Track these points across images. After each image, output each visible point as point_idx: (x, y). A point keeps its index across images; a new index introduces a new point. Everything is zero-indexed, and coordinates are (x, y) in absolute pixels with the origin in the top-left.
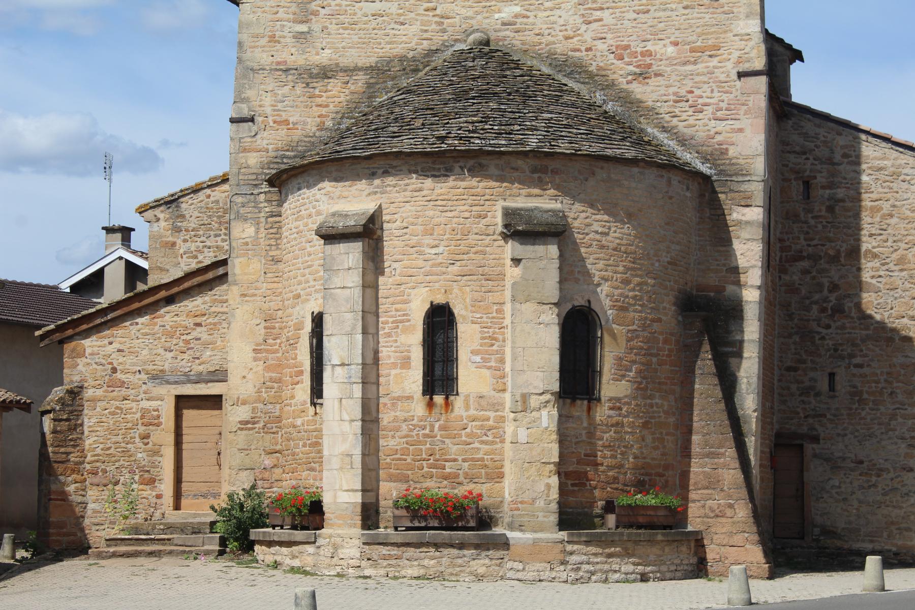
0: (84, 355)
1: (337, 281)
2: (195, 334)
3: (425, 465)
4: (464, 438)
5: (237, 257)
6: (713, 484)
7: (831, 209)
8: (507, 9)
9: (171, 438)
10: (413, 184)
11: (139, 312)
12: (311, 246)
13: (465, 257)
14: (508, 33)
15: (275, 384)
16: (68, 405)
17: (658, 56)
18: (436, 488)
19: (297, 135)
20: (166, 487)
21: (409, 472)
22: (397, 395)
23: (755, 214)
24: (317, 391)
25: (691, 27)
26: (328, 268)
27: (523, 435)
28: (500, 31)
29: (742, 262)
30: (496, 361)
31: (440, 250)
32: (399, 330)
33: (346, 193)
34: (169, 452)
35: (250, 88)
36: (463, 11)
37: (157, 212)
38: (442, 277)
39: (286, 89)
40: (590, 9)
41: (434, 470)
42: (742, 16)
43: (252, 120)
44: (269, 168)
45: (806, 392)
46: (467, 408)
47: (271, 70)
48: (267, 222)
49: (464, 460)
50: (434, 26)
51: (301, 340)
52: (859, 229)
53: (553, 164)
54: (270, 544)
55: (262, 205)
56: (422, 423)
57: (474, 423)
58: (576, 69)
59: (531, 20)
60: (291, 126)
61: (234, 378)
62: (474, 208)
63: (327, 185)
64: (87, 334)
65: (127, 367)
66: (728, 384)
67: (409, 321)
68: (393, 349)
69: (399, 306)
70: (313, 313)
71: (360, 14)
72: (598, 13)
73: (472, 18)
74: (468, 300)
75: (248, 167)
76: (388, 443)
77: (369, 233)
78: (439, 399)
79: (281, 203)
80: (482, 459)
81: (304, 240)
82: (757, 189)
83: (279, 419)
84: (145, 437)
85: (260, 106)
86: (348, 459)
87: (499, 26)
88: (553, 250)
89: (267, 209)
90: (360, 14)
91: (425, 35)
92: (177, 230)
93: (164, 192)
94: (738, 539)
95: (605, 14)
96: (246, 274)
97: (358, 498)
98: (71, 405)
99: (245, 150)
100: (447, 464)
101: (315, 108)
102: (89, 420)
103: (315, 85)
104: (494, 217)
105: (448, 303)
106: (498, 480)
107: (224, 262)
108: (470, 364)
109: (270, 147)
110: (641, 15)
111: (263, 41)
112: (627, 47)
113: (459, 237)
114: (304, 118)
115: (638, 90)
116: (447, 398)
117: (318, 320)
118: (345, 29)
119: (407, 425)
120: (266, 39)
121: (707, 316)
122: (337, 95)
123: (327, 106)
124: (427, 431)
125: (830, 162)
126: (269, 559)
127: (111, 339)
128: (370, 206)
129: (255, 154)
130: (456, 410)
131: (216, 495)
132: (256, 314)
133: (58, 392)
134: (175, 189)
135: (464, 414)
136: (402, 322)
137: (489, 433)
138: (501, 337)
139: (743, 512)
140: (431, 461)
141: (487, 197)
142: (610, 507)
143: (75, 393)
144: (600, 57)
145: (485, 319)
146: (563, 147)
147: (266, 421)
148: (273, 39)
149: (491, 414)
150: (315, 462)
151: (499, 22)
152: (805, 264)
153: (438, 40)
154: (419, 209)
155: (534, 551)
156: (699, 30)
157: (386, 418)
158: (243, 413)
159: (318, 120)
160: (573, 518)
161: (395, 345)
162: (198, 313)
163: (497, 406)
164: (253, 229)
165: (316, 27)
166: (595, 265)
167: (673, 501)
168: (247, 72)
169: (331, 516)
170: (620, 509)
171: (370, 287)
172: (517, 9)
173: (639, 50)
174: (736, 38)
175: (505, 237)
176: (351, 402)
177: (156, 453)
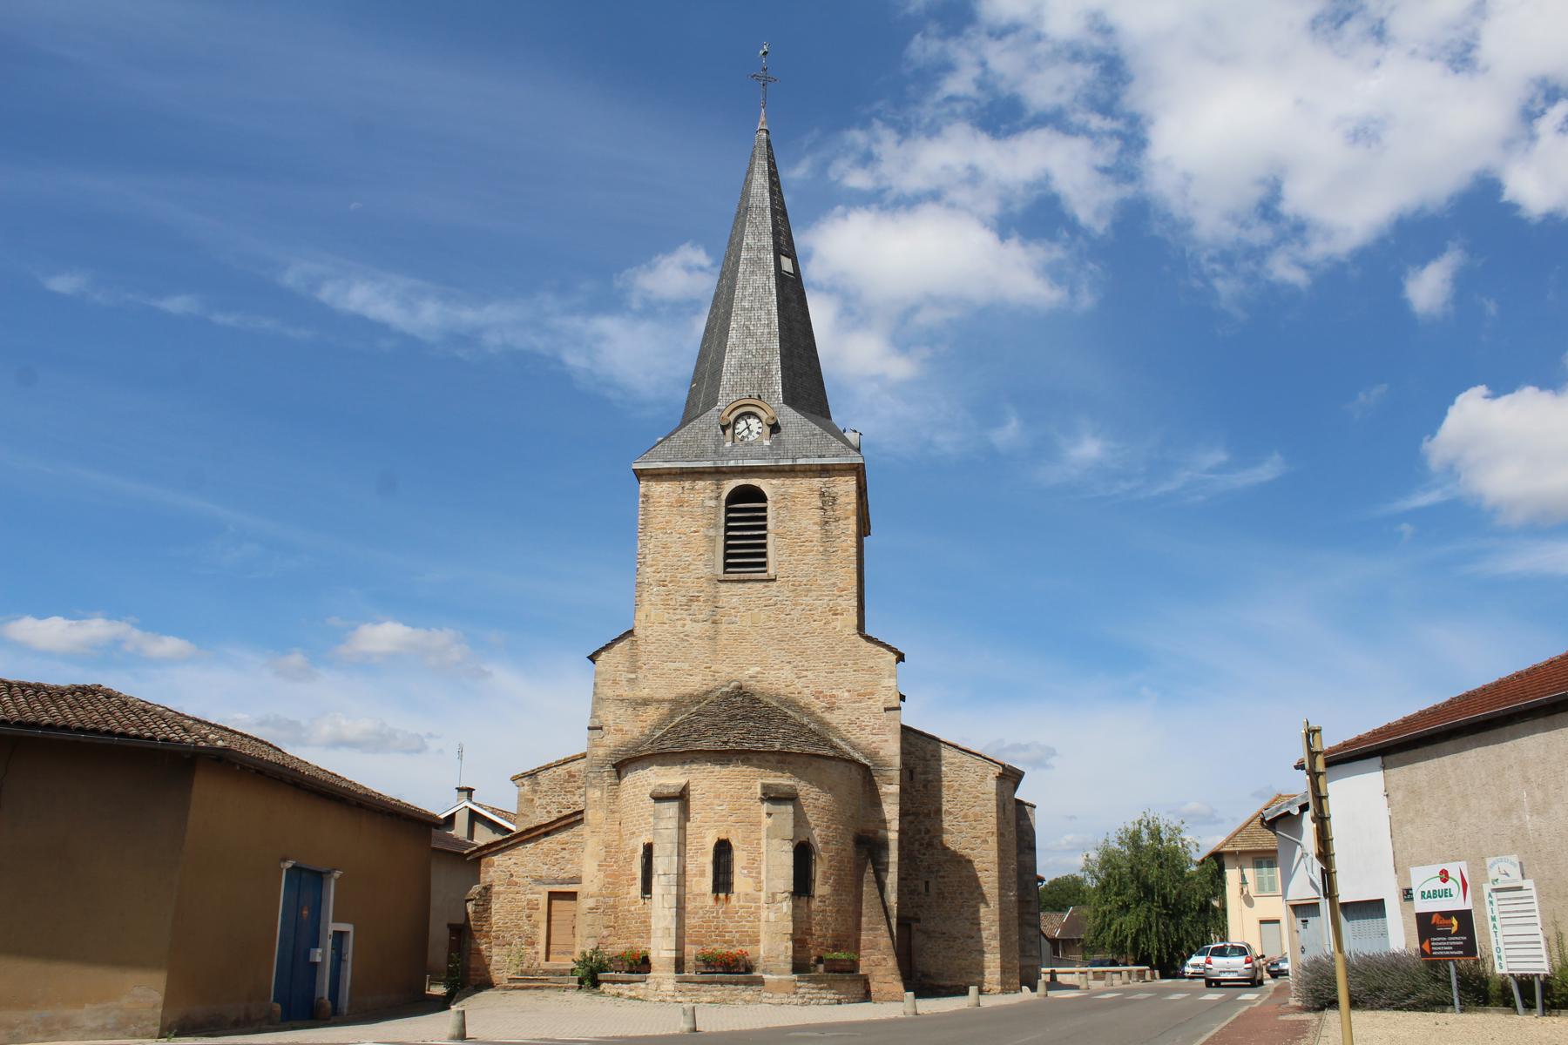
1: (662, 824)
6: (874, 946)
7: (925, 786)
9: (545, 918)
11: (528, 841)
15: (614, 882)
18: (721, 949)
19: (628, 737)
20: (541, 948)
23: (895, 789)
24: (647, 888)
27: (772, 917)
29: (888, 817)
34: (544, 926)
37: (525, 781)
45: (911, 893)
52: (940, 797)
53: (789, 759)
54: (614, 982)
58: (792, 704)
61: (585, 882)
63: (655, 768)
64: (496, 853)
66: (881, 887)
76: (691, 921)
77: (682, 796)
78: (722, 895)
79: (619, 777)
82: (896, 774)
83: (614, 907)
84: (529, 916)
88: (790, 808)
92: (535, 791)
93: (528, 769)
94: (889, 979)
95: (809, 673)
97: (673, 954)
102: (495, 906)
107: (581, 812)
114: (631, 728)
115: (828, 717)
117: (648, 849)
121: (869, 847)
122: (652, 715)
125: (925, 759)
126: (614, 991)
128: (683, 781)
131: (572, 953)
133: (476, 888)
134: (535, 767)
139: (892, 962)
142: (820, 960)
143: (487, 889)
144: (807, 698)
146: (795, 749)
147: (609, 908)
150: (646, 931)
152: (910, 818)
153: (712, 685)
155: (779, 986)
157: (689, 906)
158: (591, 903)
160: (799, 967)
163: (756, 900)
165: (641, 676)
166: (812, 818)
167: (852, 956)
168: (598, 700)
170: (825, 962)
171: (682, 828)
175: (762, 800)
177: (535, 926)
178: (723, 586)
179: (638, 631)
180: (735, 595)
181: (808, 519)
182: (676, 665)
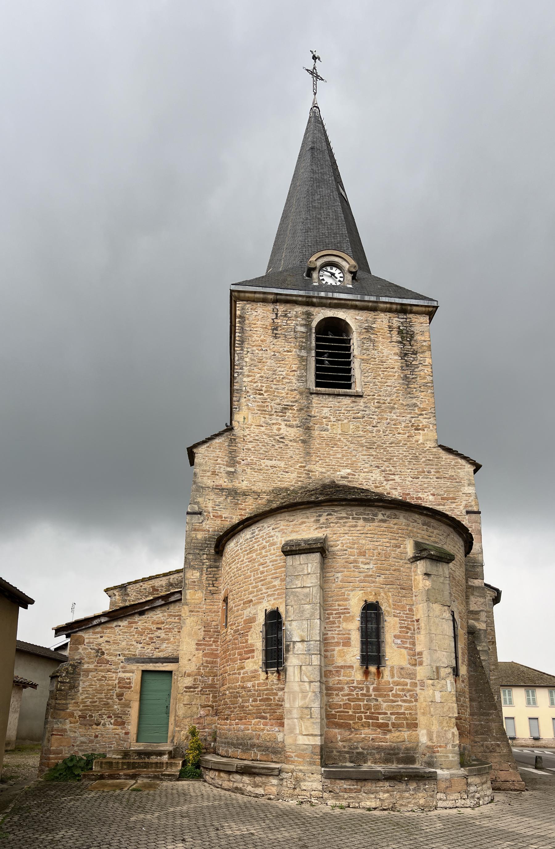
0: (83, 643)
2: (157, 634)
3: (364, 717)
4: (391, 698)
5: (188, 589)
8: (343, 471)
10: (350, 522)
12: (264, 567)
13: (387, 572)
14: (344, 482)
16: (71, 674)
17: (425, 500)
21: (351, 722)
22: (340, 665)
25: (441, 487)
26: (288, 576)
28: (340, 481)
30: (410, 644)
31: (371, 566)
32: (341, 619)
33: (298, 529)
35: (200, 497)
36: (320, 470)
38: (372, 585)
39: (222, 499)
40: (388, 474)
41: (371, 721)
42: (466, 485)
43: (200, 513)
44: (209, 541)
46: (393, 676)
47: (213, 488)
48: (207, 571)
49: (391, 714)
50: (304, 475)
51: (252, 629)
55: (205, 561)
56: (360, 686)
57: (398, 687)
59: (357, 477)
60: (223, 519)
62: (392, 541)
65: (111, 651)
67: (349, 613)
68: (336, 632)
69: (341, 603)
70: (266, 610)
71: (263, 465)
72: (393, 476)
73: (325, 473)
74: (391, 601)
75: (197, 539)
78: (373, 669)
80: (404, 714)
81: (256, 564)
85: (206, 507)
86: (306, 711)
87: (339, 479)
89: (207, 564)
90: (263, 465)
91: (299, 479)
95: (396, 477)
96: (193, 599)
98: (72, 674)
99: (195, 530)
100: (380, 716)
101: (238, 511)
103: (239, 498)
104: (405, 548)
105: (377, 602)
106: (414, 729)
108: (393, 645)
109: (211, 529)
110: (415, 479)
111: (209, 474)
112: (409, 494)
113: (383, 558)
116: (378, 668)
118: (256, 472)
119: (349, 687)
120: (210, 473)
123: (245, 510)
124: (364, 692)
127: (102, 635)
129: (201, 533)
130: (385, 677)
132: (199, 623)
135: (391, 680)
136: (343, 613)
137: (407, 695)
138: (412, 628)
140: (368, 714)
141: (400, 535)
145: (401, 614)
148: (214, 473)
149: (409, 681)
151: (340, 476)
154: (355, 538)
156: (445, 489)
159: (240, 517)
161: (338, 629)
162: (160, 621)
163: (412, 675)
164: (198, 574)
169: (293, 755)
172: (349, 471)
173: (415, 496)
174: (464, 495)
176: (310, 668)
178: (315, 399)
179: (237, 431)
180: (326, 407)
181: (389, 351)
182: (273, 463)
